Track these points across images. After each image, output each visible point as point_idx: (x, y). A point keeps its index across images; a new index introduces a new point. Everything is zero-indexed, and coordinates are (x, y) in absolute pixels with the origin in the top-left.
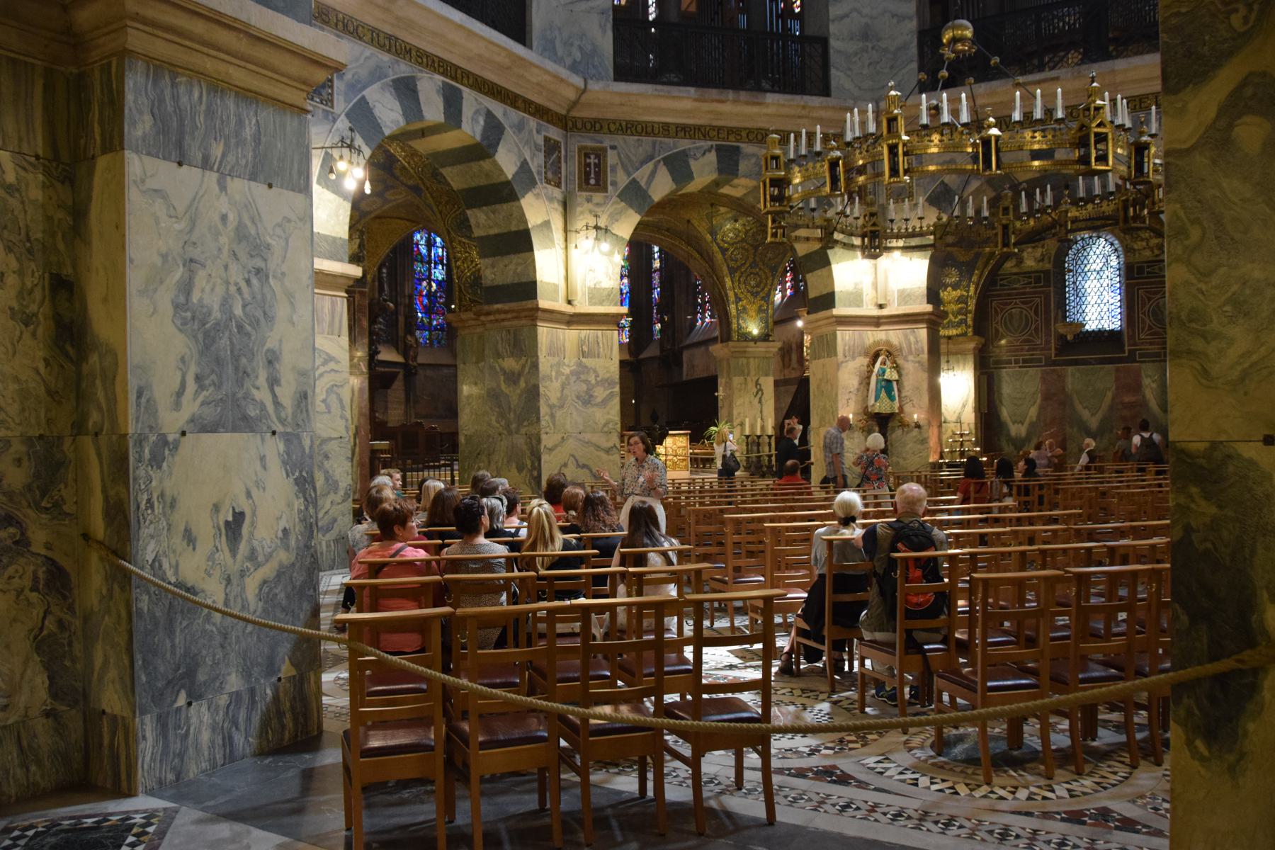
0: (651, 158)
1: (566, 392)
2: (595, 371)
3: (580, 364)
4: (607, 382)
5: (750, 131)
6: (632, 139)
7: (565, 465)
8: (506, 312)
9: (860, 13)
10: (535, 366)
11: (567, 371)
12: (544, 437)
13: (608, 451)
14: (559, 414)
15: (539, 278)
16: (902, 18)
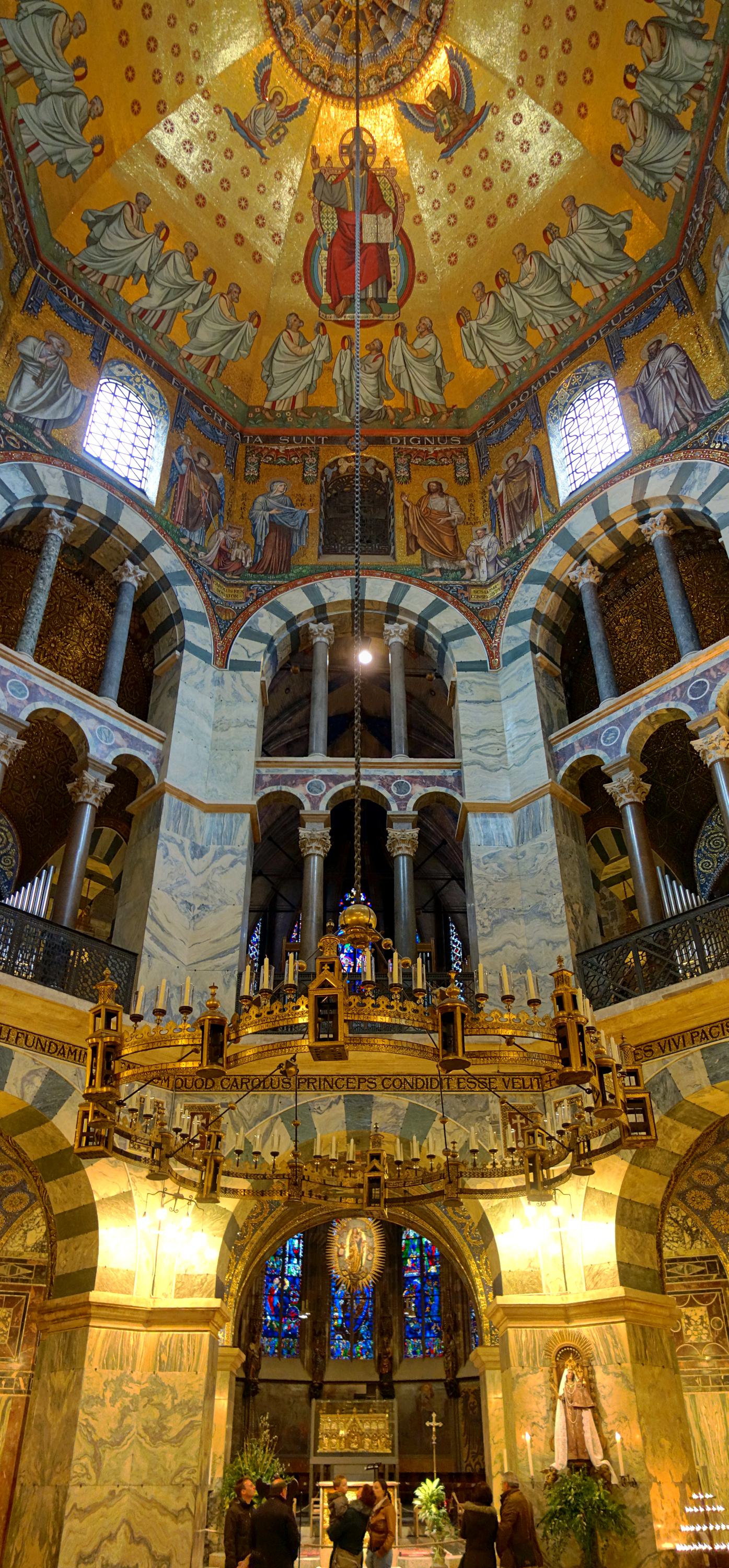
0: (266, 1114)
1: (128, 1421)
2: (173, 1390)
3: (155, 1381)
4: (188, 1408)
5: (384, 1077)
7: (111, 1537)
8: (64, 1309)
9: (514, 944)
10: (79, 1383)
11: (135, 1390)
12: (74, 1491)
13: (176, 1516)
14: (108, 1456)
15: (101, 1263)
16: (555, 944)
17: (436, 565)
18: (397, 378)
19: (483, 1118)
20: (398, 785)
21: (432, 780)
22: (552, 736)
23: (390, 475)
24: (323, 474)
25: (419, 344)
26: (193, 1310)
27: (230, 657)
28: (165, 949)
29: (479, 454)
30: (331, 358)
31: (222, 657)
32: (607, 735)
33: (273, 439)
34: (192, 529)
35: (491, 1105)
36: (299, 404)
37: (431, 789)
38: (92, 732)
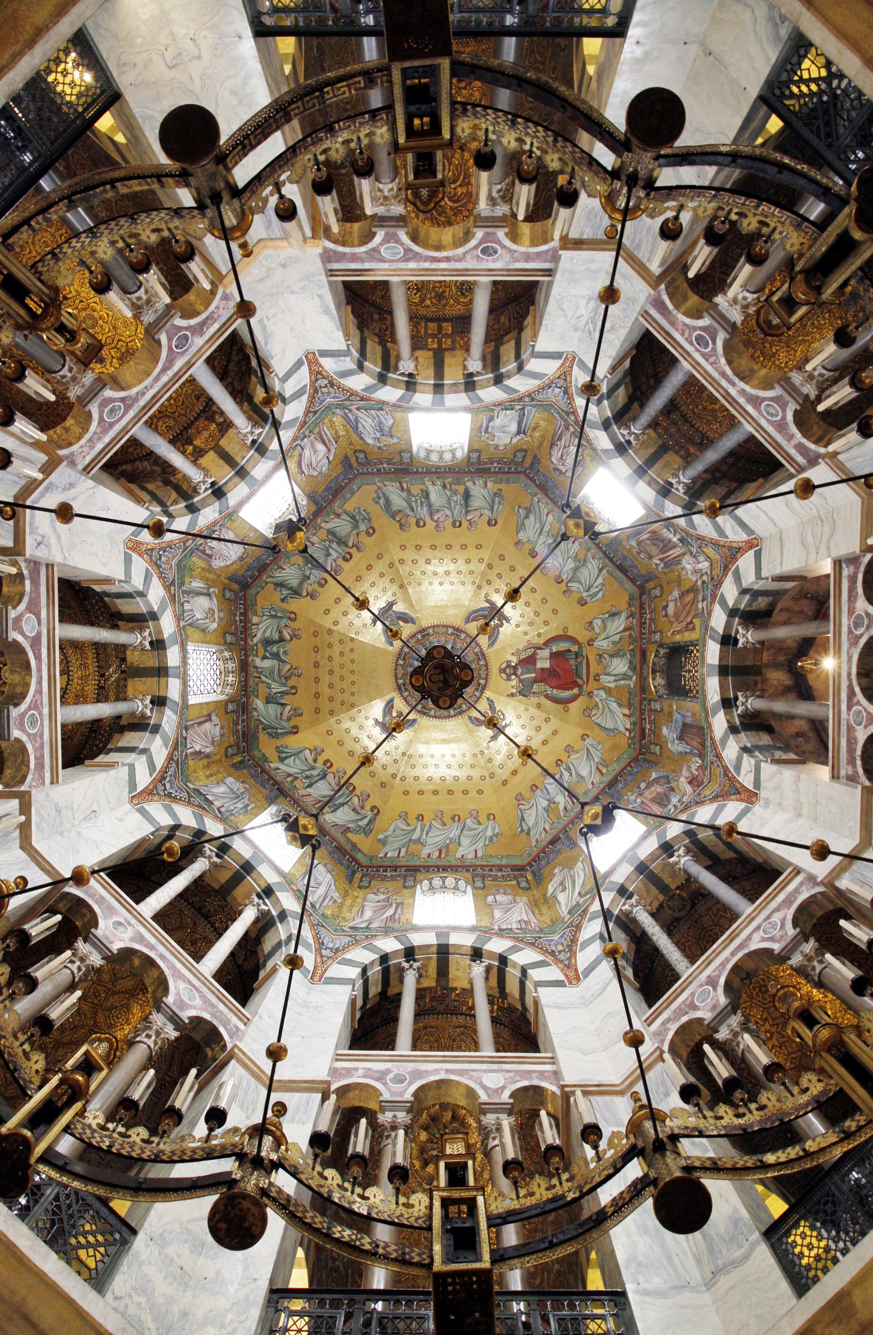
17: (700, 606)
18: (614, 643)
20: (857, 625)
21: (852, 589)
22: (793, 471)
23: (661, 646)
24: (660, 697)
25: (597, 630)
27: (751, 787)
29: (647, 581)
30: (604, 688)
31: (750, 797)
32: (772, 415)
33: (643, 731)
34: (669, 801)
36: (627, 712)
37: (860, 590)
38: (763, 940)
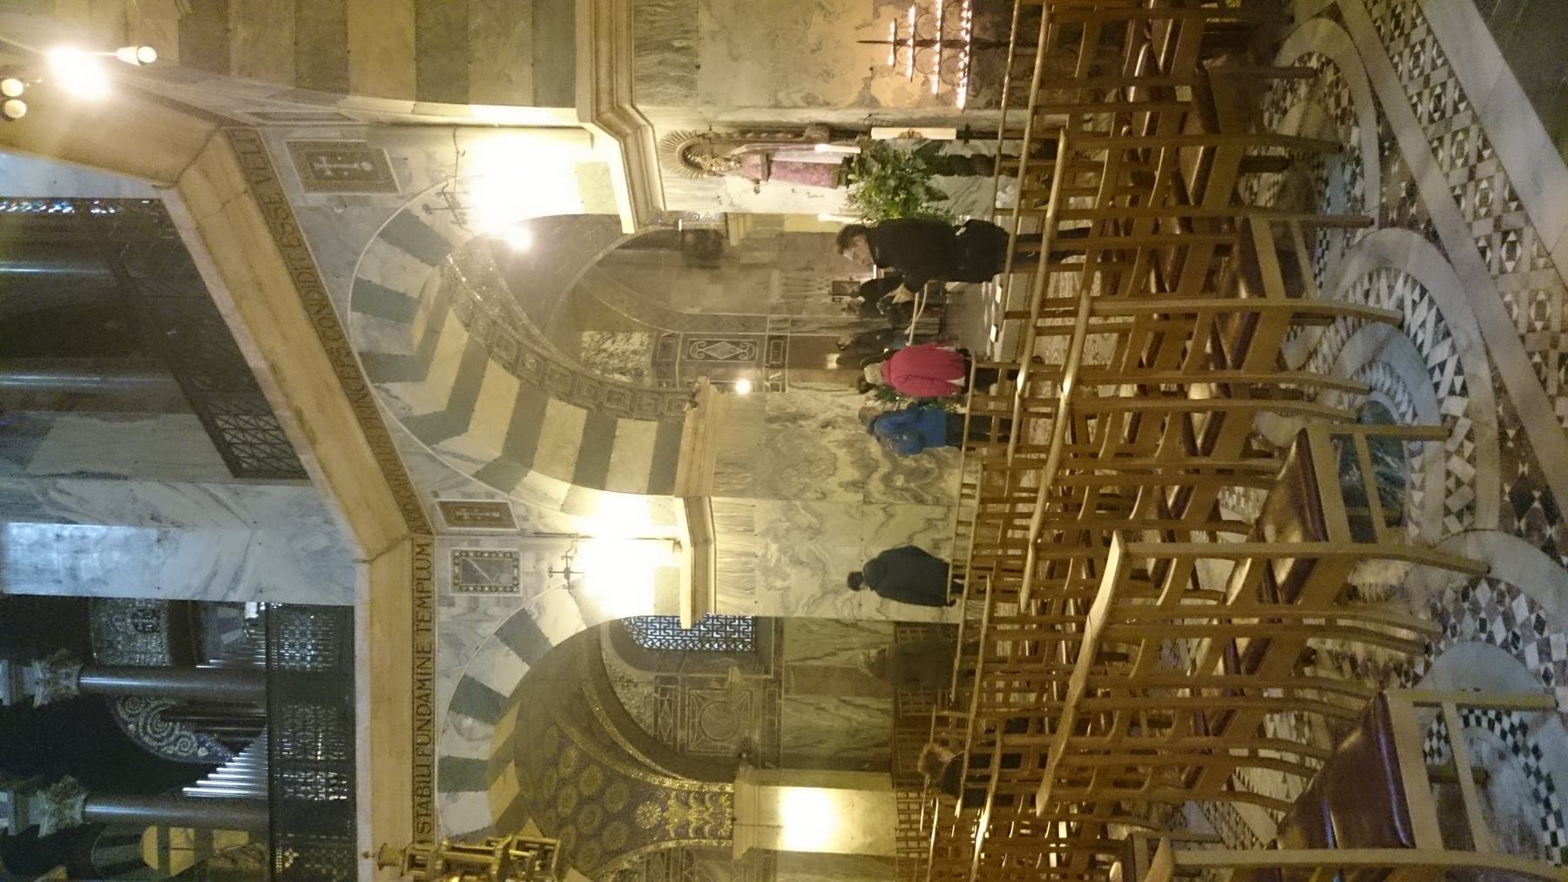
0: (432, 459)
1: (804, 559)
3: (764, 534)
6: (413, 478)
11: (774, 547)
19: (340, 217)
26: (689, 516)
28: (241, 569)
35: (311, 203)
